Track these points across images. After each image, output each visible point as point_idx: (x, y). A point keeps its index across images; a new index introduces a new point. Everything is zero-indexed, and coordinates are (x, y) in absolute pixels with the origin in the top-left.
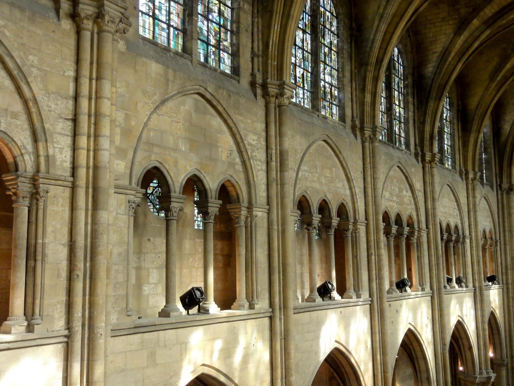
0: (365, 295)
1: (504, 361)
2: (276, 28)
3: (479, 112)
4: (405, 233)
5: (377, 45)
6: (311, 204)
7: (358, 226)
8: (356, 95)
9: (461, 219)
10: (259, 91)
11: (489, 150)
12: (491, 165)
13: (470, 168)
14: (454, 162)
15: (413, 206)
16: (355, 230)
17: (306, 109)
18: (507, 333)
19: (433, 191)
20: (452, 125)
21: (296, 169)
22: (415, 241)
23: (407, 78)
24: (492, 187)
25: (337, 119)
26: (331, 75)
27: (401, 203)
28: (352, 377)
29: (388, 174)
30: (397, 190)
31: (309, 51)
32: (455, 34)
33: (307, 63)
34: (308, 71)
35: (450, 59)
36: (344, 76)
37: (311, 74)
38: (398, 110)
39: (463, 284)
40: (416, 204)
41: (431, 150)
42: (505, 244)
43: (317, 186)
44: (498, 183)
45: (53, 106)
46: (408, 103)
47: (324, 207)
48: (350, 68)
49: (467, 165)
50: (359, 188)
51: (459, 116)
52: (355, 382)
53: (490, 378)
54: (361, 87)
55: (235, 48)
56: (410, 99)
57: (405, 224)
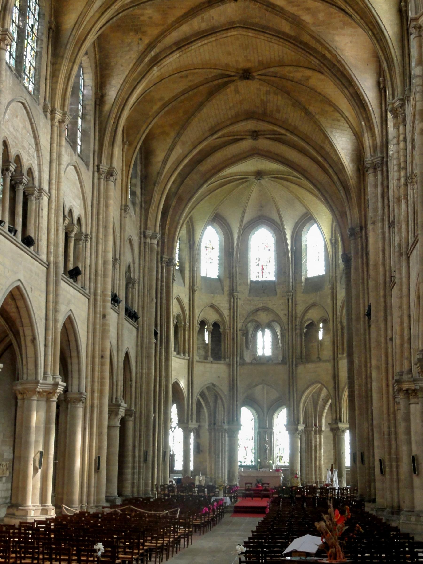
1: (81, 393)
11: (88, 117)
12: (89, 137)
13: (58, 105)
18: (90, 359)
20: (39, 42)
42: (97, 243)
44: (96, 163)
49: (55, 101)
51: (51, 35)
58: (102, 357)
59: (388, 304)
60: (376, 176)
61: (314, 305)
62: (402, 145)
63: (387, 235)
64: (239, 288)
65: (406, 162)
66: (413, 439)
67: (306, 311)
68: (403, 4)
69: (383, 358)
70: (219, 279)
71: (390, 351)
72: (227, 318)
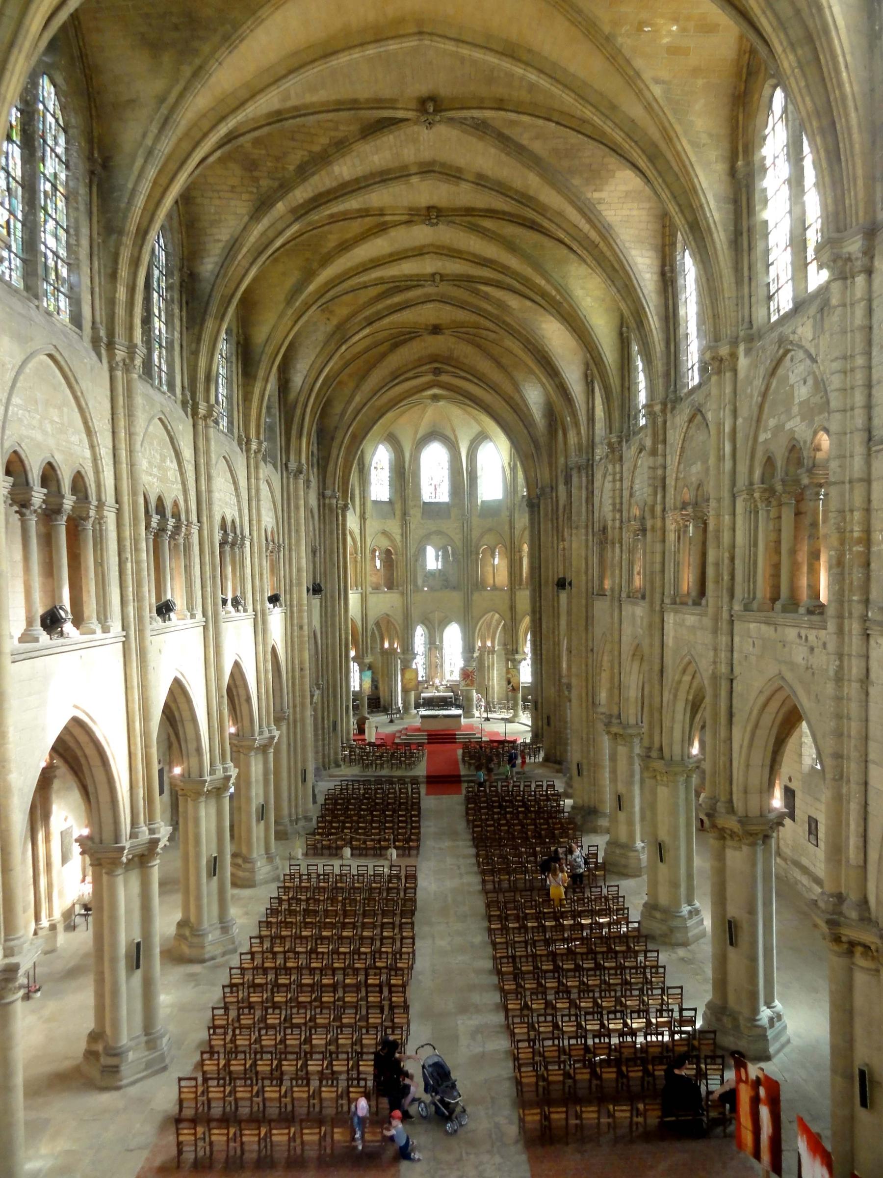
0: (116, 626)
3: (270, 350)
4: (170, 527)
5: (140, 201)
6: (28, 468)
7: (105, 513)
9: (240, 510)
14: (231, 422)
15: (180, 486)
16: (100, 520)
17: (16, 291)
19: (208, 464)
21: (4, 401)
22: (182, 541)
23: (172, 274)
24: (275, 467)
26: (56, 236)
27: (163, 479)
28: (95, 761)
29: (147, 429)
30: (158, 457)
31: (19, 179)
32: (251, 218)
33: (14, 201)
34: (16, 217)
35: (240, 257)
36: (78, 245)
37: (24, 225)
38: (159, 325)
39: (240, 608)
40: (184, 484)
41: (207, 400)
42: (290, 550)
43: (38, 436)
46: (173, 315)
47: (49, 475)
48: (88, 233)
52: (101, 769)
53: (273, 738)
54: (109, 271)
56: (177, 311)
57: (169, 513)
58: (302, 669)
59: (590, 614)
60: (580, 477)
61: (490, 530)
62: (618, 484)
63: (590, 543)
64: (412, 512)
65: (621, 504)
66: (619, 778)
67: (482, 536)
68: (624, 329)
69: (583, 667)
70: (391, 502)
71: (590, 661)
72: (400, 544)
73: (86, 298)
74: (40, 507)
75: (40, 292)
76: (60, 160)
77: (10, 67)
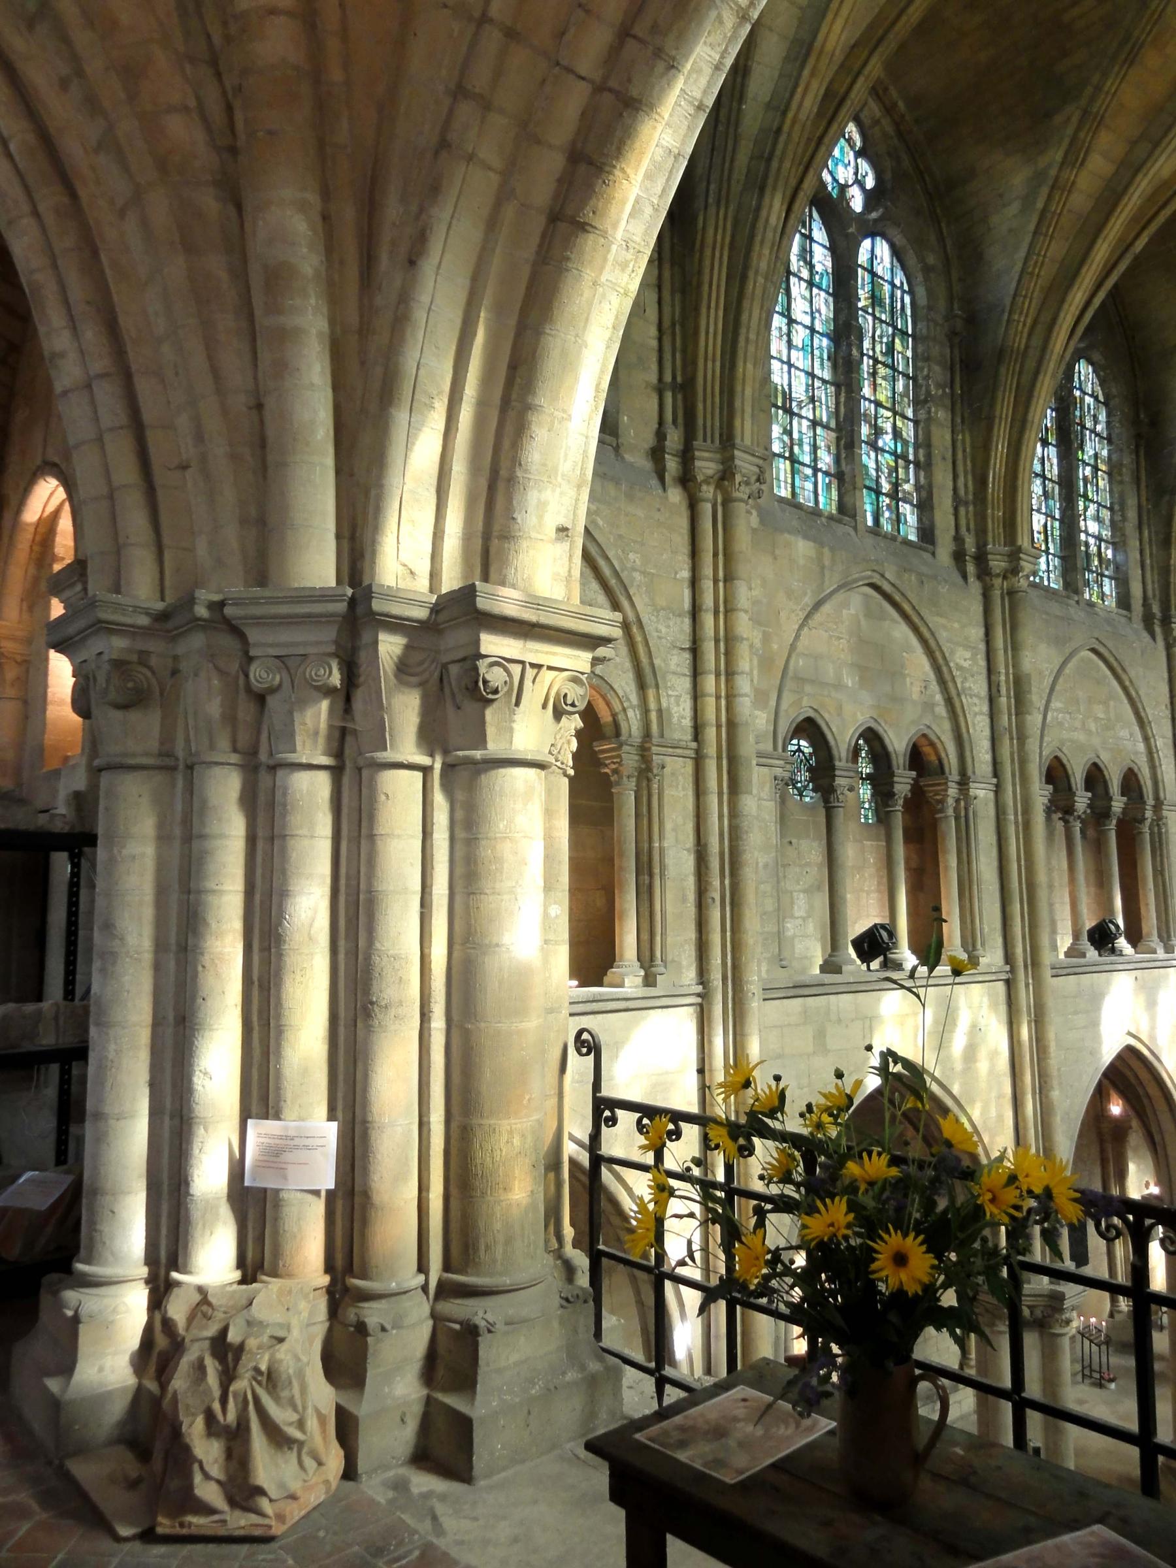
2: (1000, 448)
6: (1070, 772)
7: (1165, 813)
8: (1151, 554)
10: (971, 568)
17: (1054, 592)
25: (1114, 605)
26: (1097, 519)
31: (1055, 478)
34: (1053, 518)
36: (1124, 518)
37: (1061, 521)
43: (1081, 737)
45: (664, 630)
47: (1095, 777)
48: (1136, 502)
50: (1163, 737)
55: (924, 494)
73: (1135, 575)
74: (1085, 812)
75: (1080, 584)
76: (1102, 438)
77: (1036, 394)
